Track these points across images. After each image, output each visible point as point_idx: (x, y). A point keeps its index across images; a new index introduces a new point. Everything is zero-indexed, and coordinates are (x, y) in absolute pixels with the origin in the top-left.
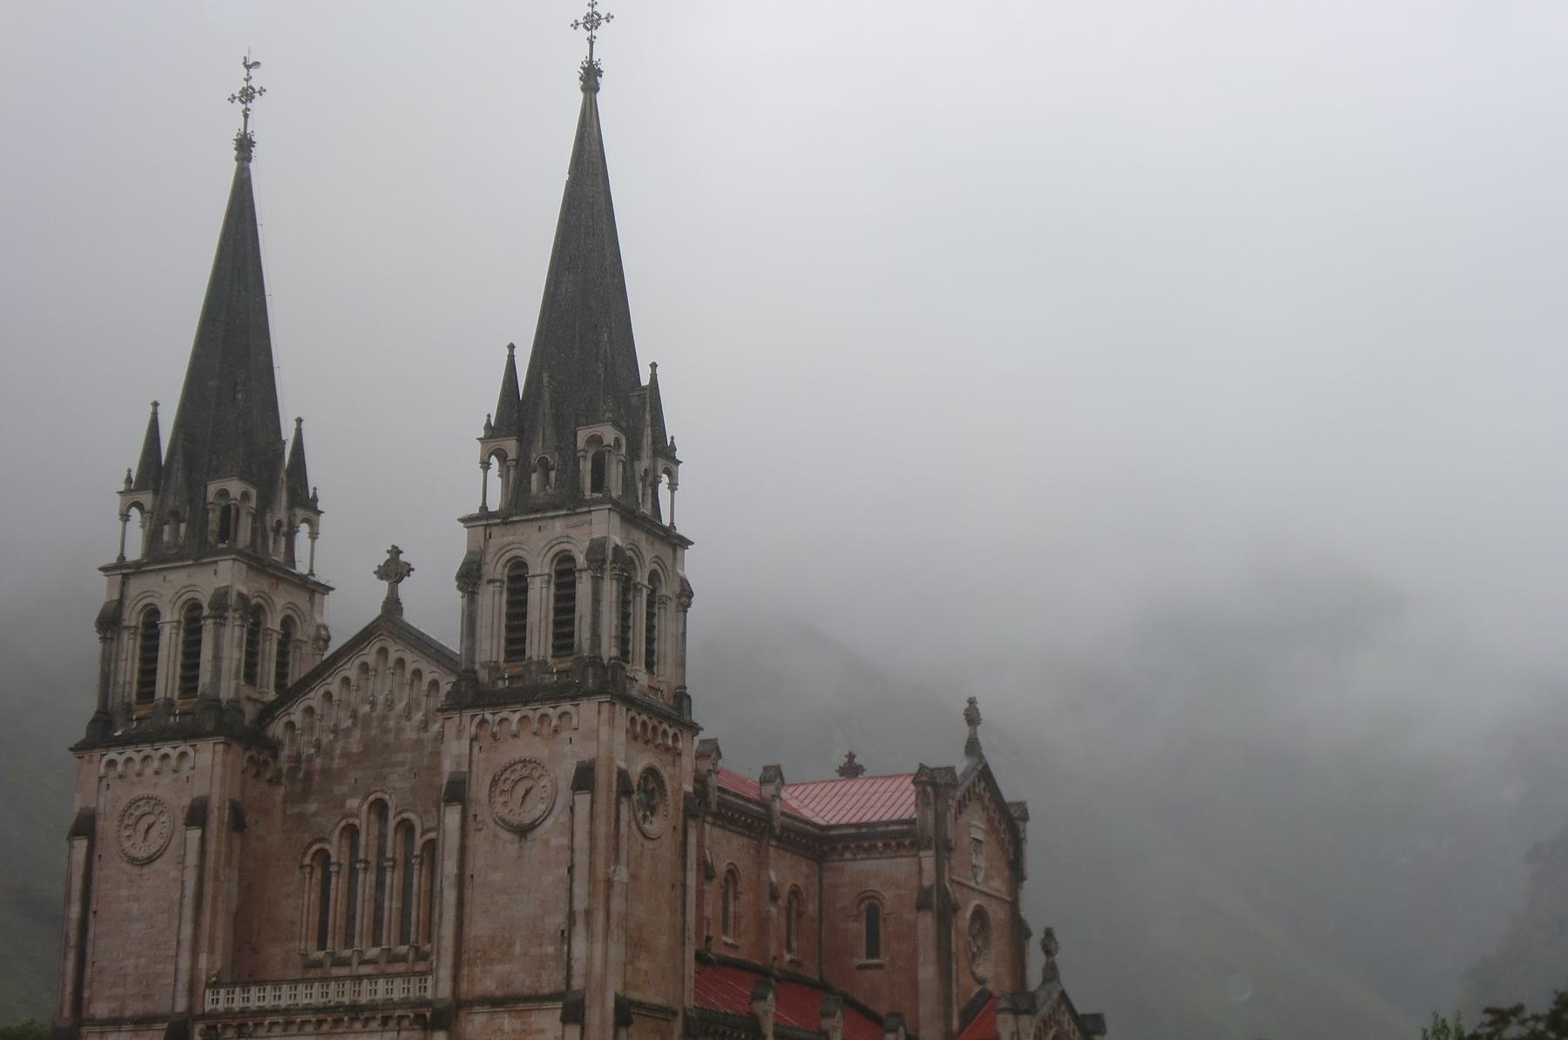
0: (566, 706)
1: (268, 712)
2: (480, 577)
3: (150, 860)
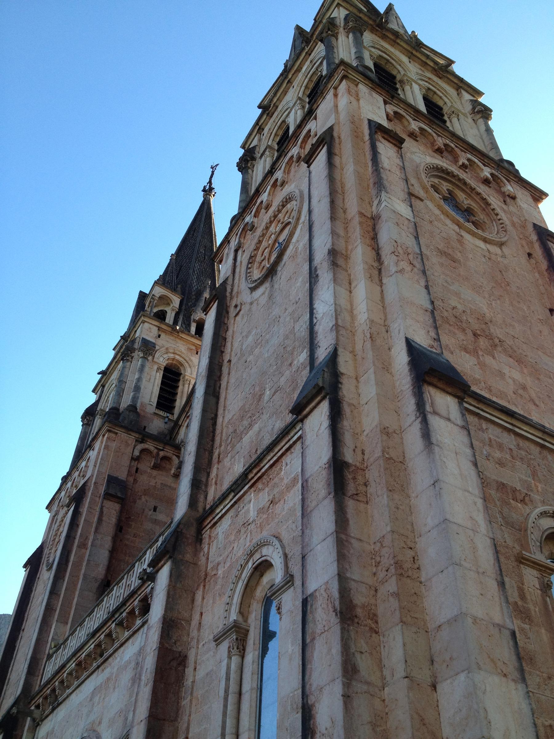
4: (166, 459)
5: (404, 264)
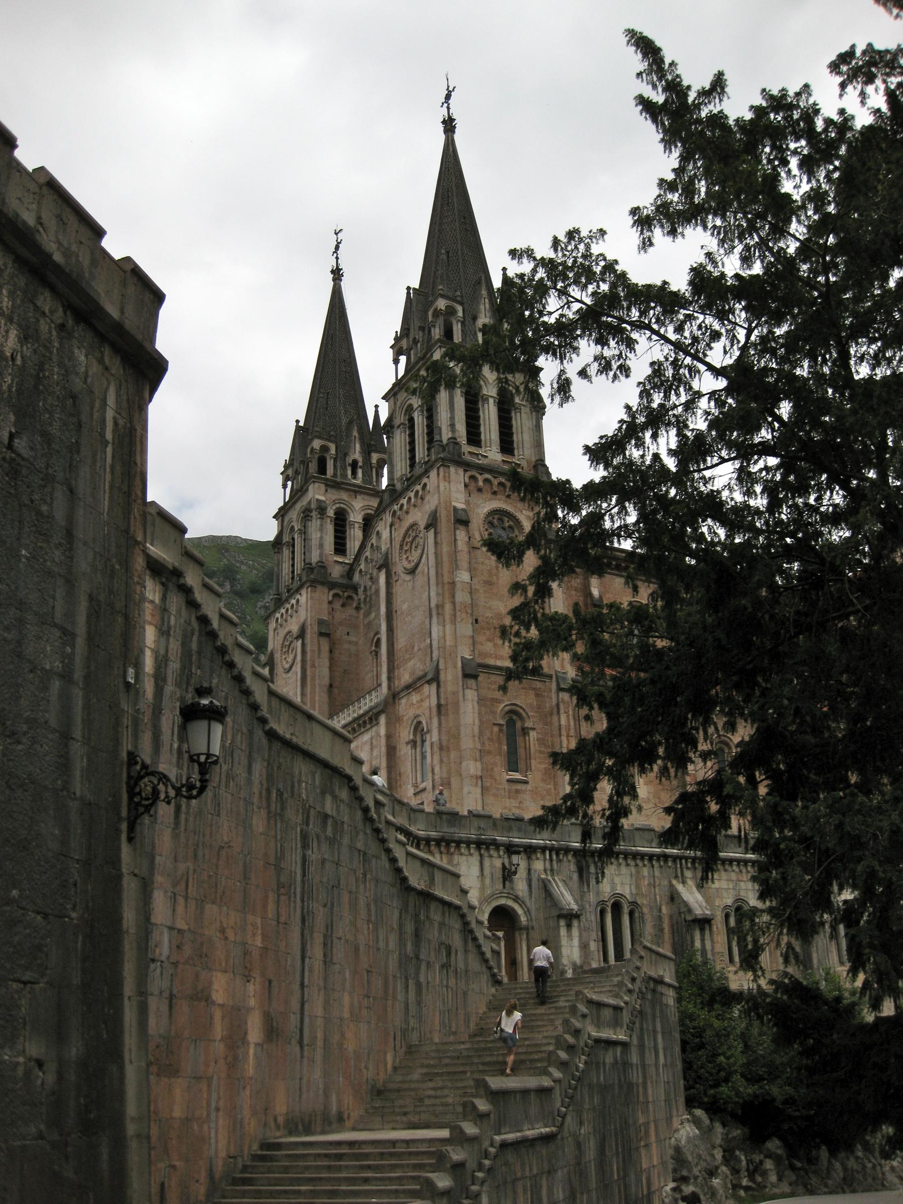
0: (425, 480)
1: (351, 570)
2: (392, 427)
3: (291, 668)
4: (350, 597)
5: (464, 615)
